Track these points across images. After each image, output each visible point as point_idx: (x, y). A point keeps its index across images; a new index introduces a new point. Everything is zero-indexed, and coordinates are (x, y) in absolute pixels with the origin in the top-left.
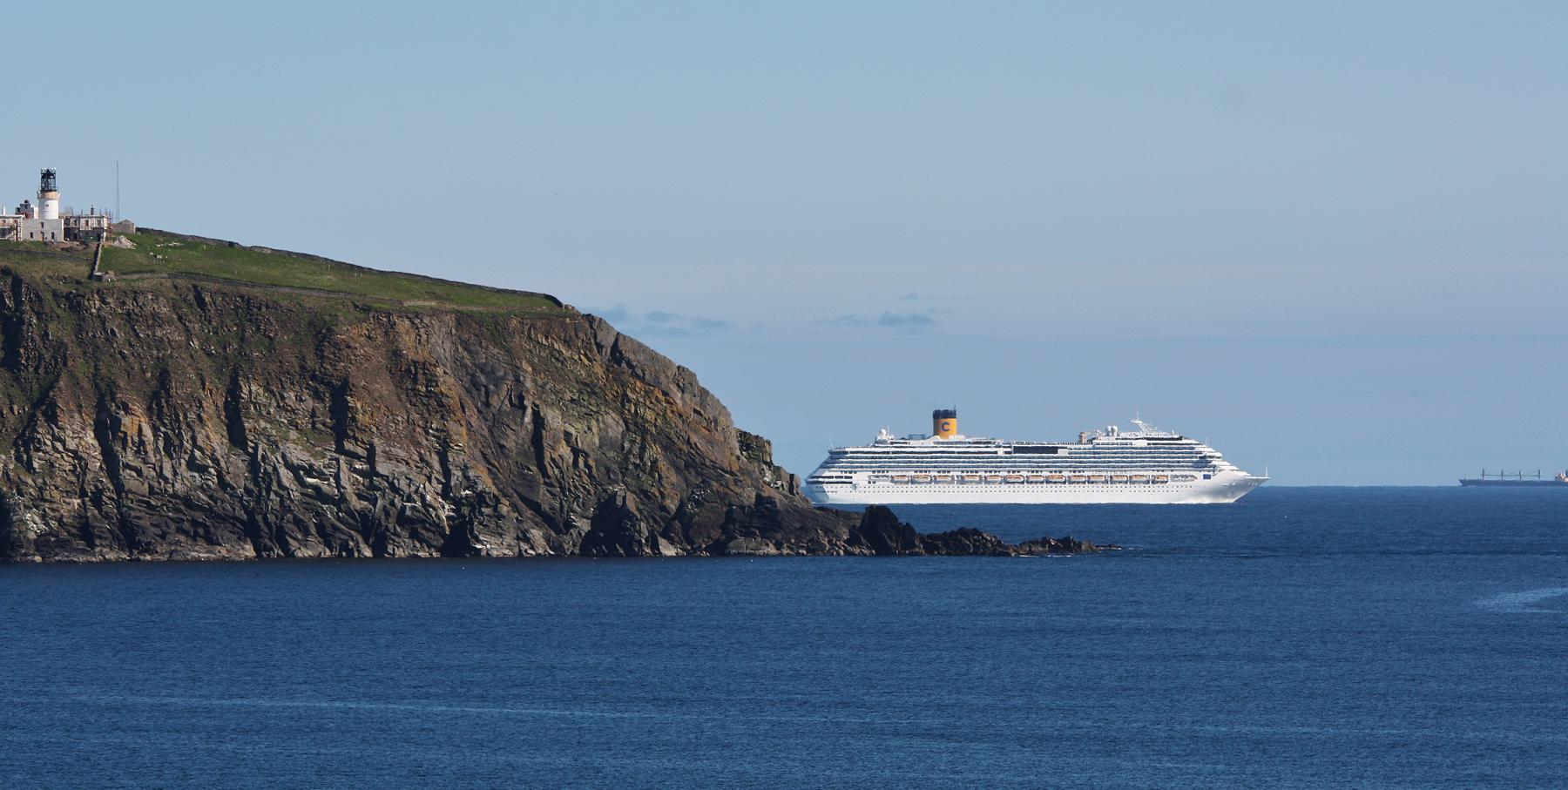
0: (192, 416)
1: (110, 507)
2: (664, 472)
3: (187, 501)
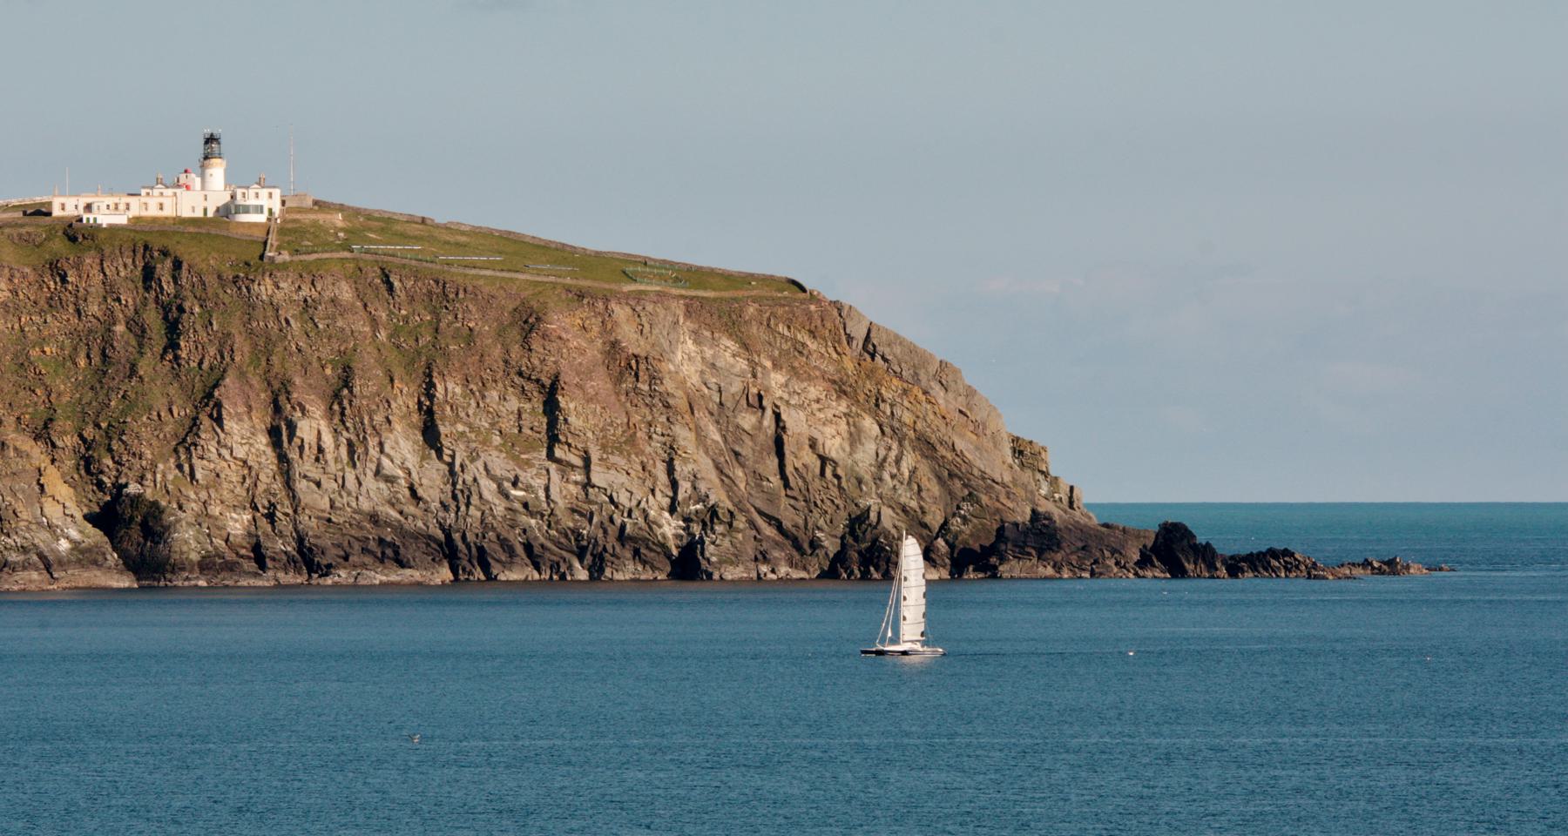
0: (379, 418)
1: (284, 524)
2: (925, 483)
3: (374, 518)
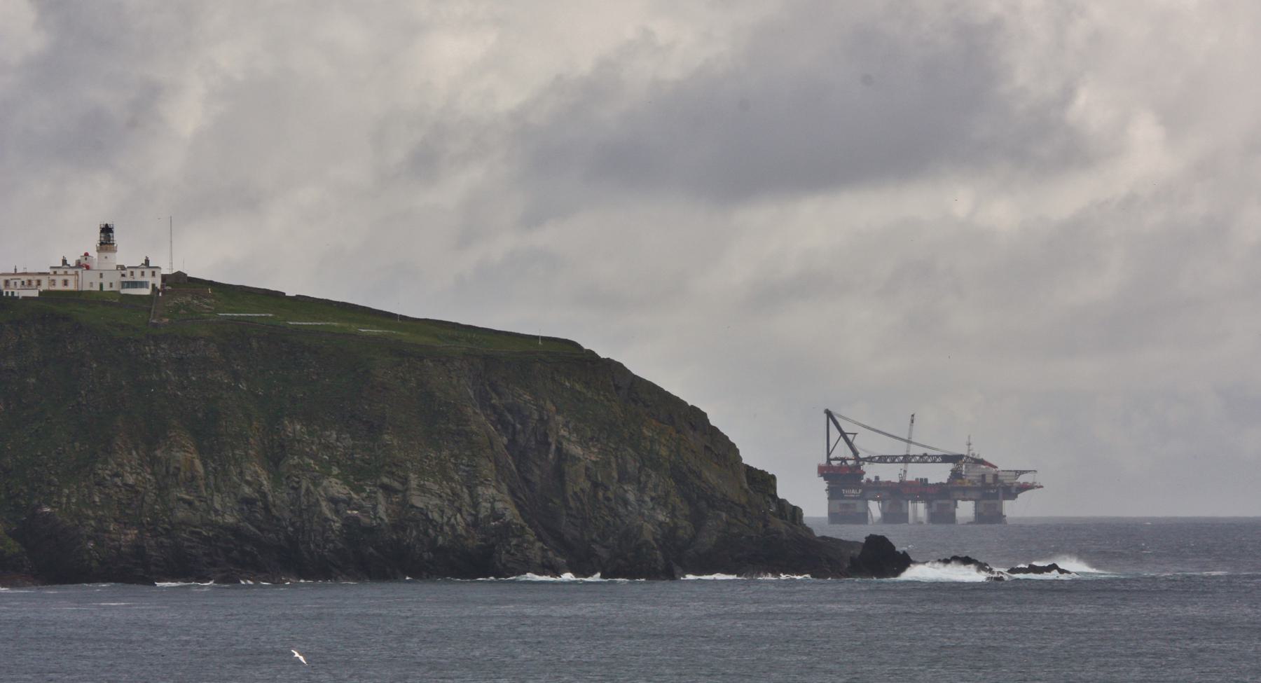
3: (235, 531)
